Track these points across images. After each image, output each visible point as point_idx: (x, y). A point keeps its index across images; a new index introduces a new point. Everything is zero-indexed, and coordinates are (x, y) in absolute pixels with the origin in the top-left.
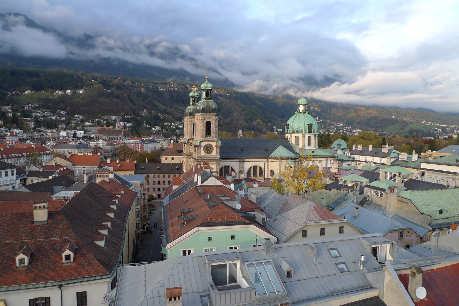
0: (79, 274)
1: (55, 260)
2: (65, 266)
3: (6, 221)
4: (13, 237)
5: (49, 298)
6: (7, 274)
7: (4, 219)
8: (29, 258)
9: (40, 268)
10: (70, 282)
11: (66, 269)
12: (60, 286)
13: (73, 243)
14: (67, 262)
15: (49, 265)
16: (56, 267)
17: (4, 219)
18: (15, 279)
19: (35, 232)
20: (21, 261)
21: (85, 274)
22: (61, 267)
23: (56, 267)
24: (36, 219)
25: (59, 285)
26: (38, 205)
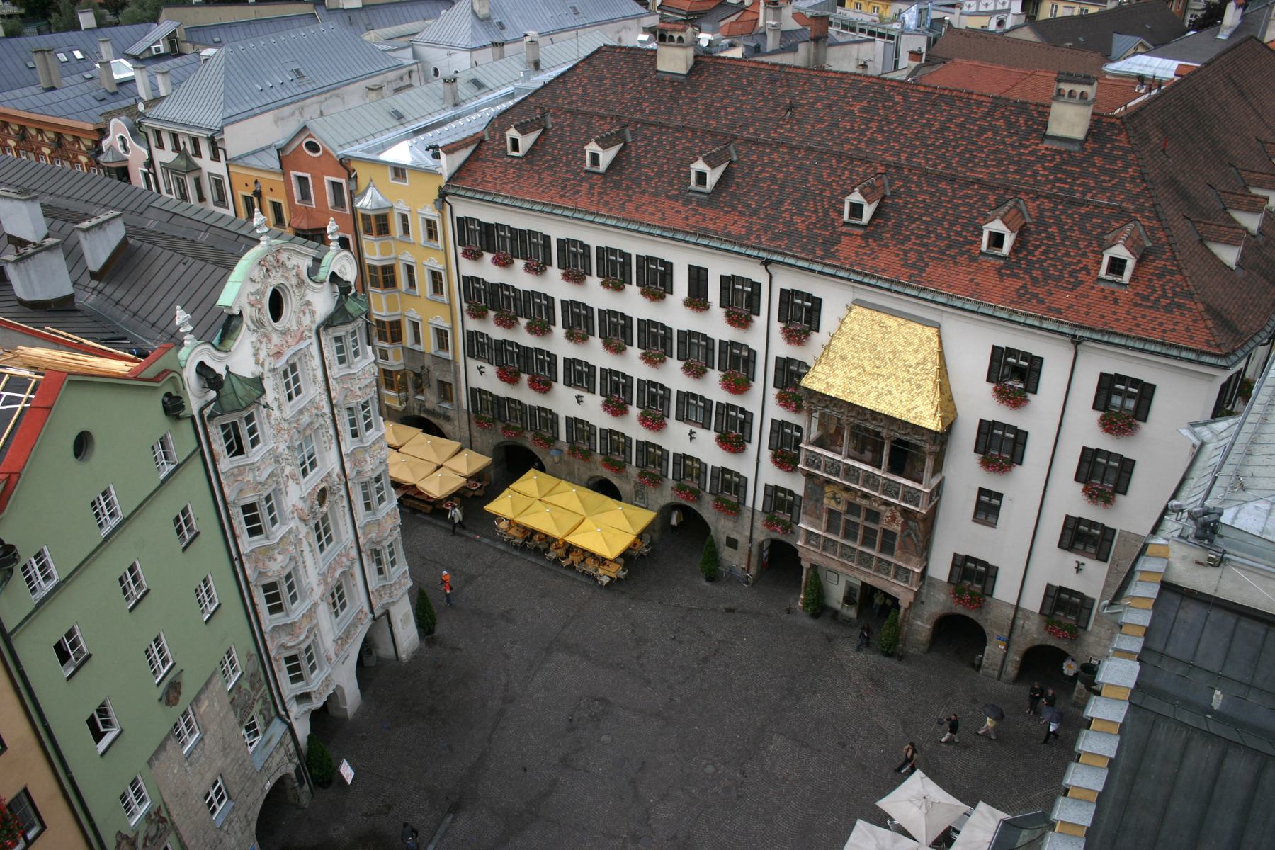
0: (1138, 325)
1: (1080, 262)
2: (1103, 290)
3: (978, 119)
4: (986, 166)
5: (1042, 359)
6: (955, 263)
7: (972, 112)
8: (1014, 235)
9: (1037, 274)
10: (1106, 339)
11: (1105, 298)
12: (1076, 342)
13: (1141, 230)
14: (1110, 278)
15: (1061, 271)
16: (1079, 283)
17: (972, 112)
18: (971, 280)
19: (1045, 169)
20: (997, 240)
21: (1154, 329)
22: (1093, 288)
23: (1079, 283)
24: (1054, 129)
25: (1074, 336)
26: (1067, 88)
